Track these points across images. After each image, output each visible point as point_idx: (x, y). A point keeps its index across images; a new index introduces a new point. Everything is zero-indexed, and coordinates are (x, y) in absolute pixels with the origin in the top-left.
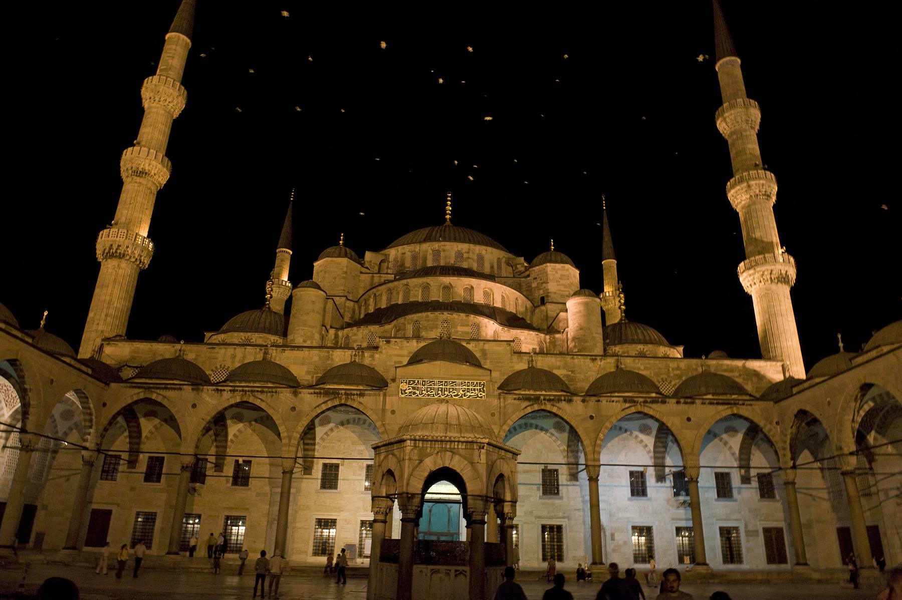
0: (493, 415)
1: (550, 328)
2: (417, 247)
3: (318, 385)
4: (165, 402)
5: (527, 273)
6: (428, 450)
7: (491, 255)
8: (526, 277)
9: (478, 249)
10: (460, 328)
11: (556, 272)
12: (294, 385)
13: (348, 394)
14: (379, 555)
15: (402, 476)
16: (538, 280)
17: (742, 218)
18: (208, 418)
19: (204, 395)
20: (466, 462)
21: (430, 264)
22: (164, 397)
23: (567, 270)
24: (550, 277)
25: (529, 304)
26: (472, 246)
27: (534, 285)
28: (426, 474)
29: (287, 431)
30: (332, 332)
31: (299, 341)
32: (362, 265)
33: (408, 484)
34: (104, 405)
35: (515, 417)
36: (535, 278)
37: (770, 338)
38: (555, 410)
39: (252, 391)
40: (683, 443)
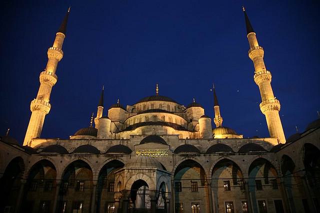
0: (171, 162)
1: (193, 130)
2: (145, 103)
3: (106, 154)
4: (51, 161)
7: (172, 105)
9: (167, 103)
10: (159, 131)
12: (97, 152)
13: (117, 156)
15: (123, 184)
17: (260, 88)
18: (66, 166)
19: (65, 158)
21: (150, 108)
22: (51, 159)
25: (186, 122)
26: (165, 102)
30: (114, 134)
31: (101, 137)
32: (126, 110)
33: (126, 186)
34: (29, 162)
35: (179, 162)
37: (273, 130)
38: (194, 159)
40: (242, 169)
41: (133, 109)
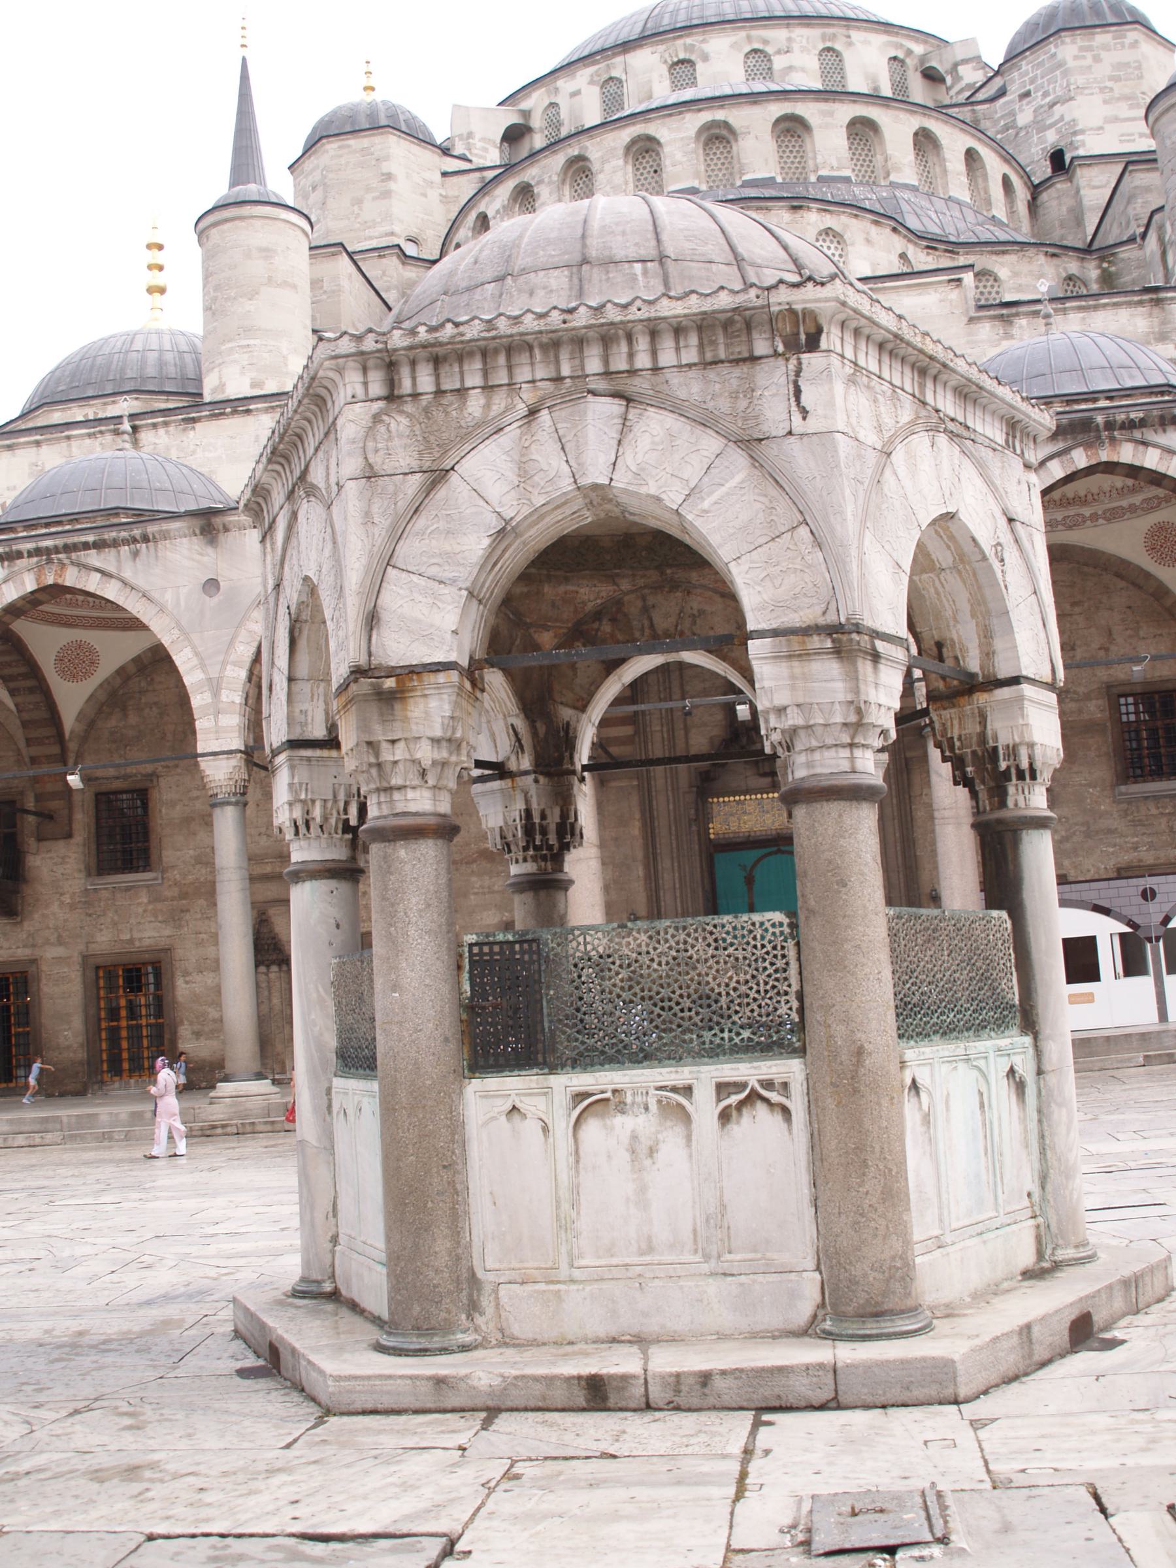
5: (998, 82)
6: (475, 404)
8: (992, 100)
11: (1097, 59)
14: (332, 1042)
16: (1038, 100)
20: (711, 443)
23: (1135, 44)
24: (1080, 80)
27: (1024, 117)
28: (476, 545)
29: (203, 666)
33: (372, 620)
36: (1027, 94)
38: (1151, 460)
39: (68, 549)
41: (514, 135)
